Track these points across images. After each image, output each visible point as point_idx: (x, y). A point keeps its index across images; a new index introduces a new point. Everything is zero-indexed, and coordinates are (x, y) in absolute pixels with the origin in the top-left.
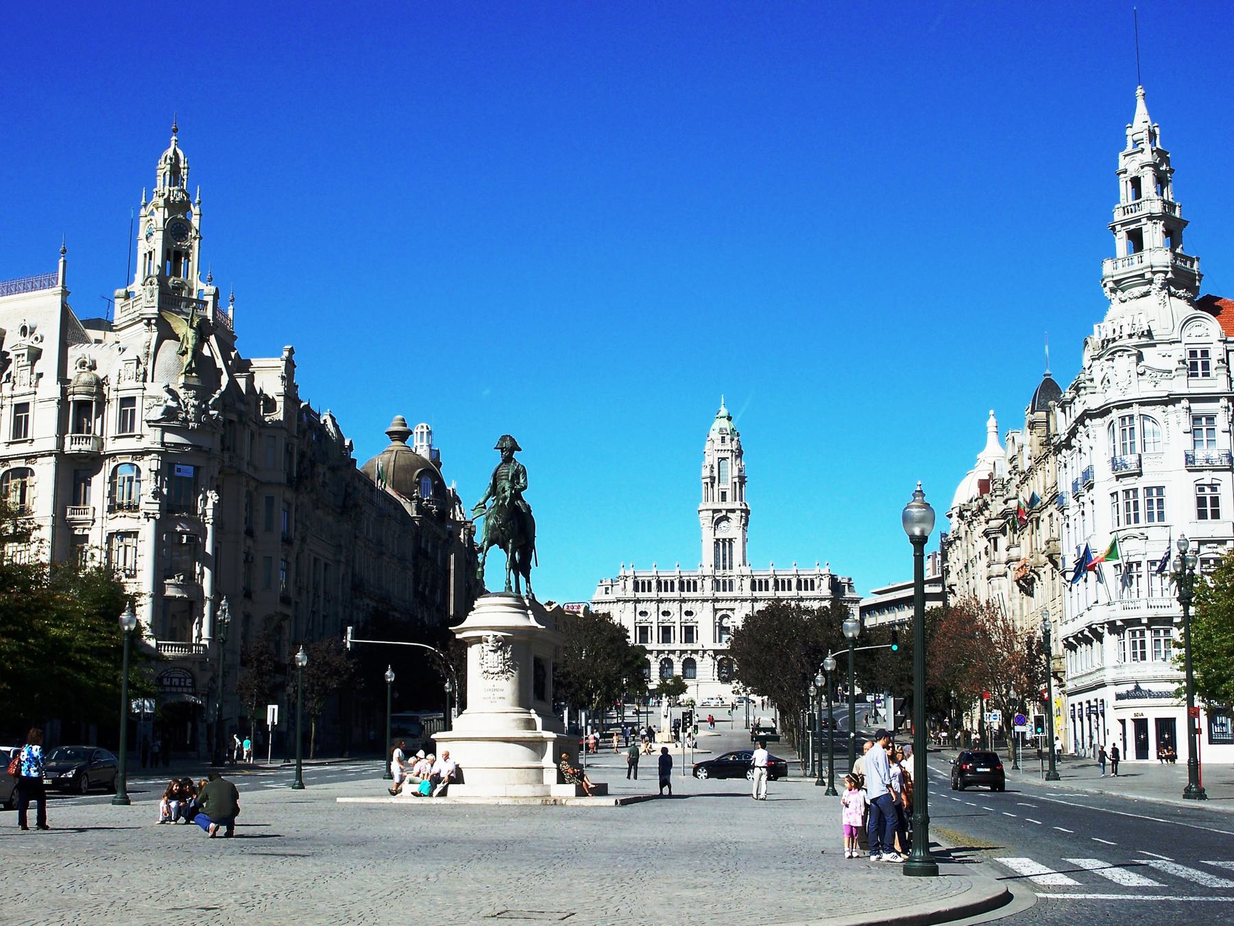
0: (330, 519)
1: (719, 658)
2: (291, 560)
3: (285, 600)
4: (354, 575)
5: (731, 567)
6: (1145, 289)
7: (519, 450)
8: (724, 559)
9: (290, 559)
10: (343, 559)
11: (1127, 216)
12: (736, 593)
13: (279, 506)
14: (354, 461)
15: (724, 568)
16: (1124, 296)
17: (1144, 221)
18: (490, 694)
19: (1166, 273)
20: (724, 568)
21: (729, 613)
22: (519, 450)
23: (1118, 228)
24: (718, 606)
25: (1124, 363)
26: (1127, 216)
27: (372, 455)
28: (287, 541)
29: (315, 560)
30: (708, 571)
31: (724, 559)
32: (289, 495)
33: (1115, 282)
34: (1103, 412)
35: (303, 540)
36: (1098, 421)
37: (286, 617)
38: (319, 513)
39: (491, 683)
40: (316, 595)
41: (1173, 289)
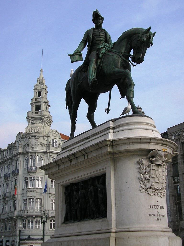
6: (41, 121)
11: (36, 101)
16: (33, 122)
17: (42, 103)
19: (47, 118)
23: (33, 104)
25: (33, 141)
26: (36, 101)
33: (32, 118)
34: (25, 154)
36: (23, 156)
41: (47, 123)
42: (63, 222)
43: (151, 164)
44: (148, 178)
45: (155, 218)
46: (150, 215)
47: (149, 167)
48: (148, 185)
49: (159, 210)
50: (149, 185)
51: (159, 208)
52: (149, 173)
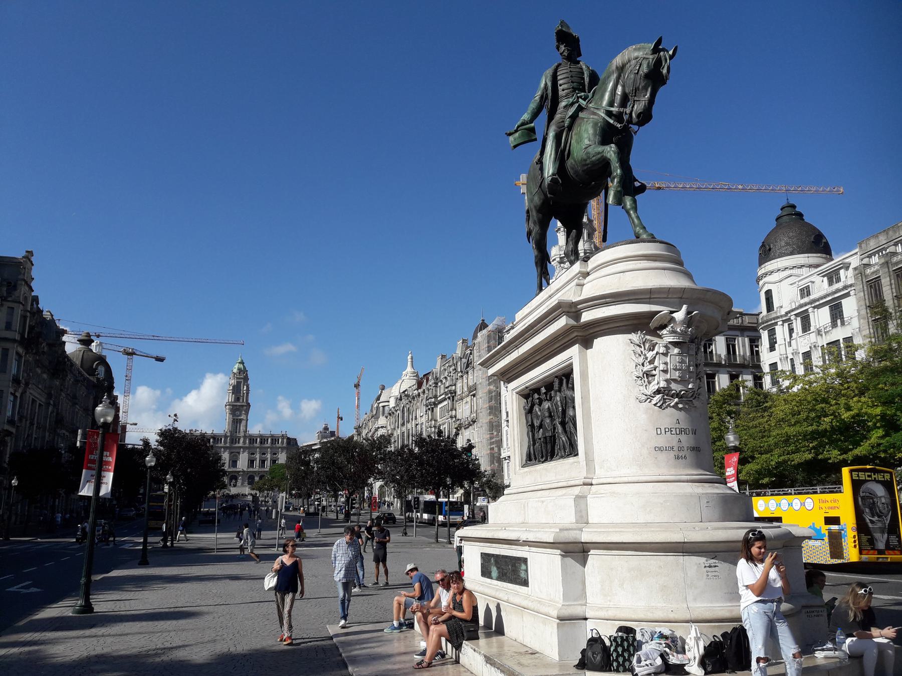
0: (45, 376)
2: (18, 394)
3: (11, 422)
4: (57, 414)
9: (18, 394)
10: (52, 402)
12: (241, 444)
13: (13, 356)
14: (64, 342)
27: (71, 346)
28: (16, 381)
29: (33, 401)
30: (228, 434)
32: (20, 350)
35: (27, 384)
37: (9, 433)
38: (39, 371)
40: (32, 424)
42: (524, 462)
44: (654, 372)
46: (660, 449)
48: (654, 387)
50: (657, 387)
52: (652, 362)
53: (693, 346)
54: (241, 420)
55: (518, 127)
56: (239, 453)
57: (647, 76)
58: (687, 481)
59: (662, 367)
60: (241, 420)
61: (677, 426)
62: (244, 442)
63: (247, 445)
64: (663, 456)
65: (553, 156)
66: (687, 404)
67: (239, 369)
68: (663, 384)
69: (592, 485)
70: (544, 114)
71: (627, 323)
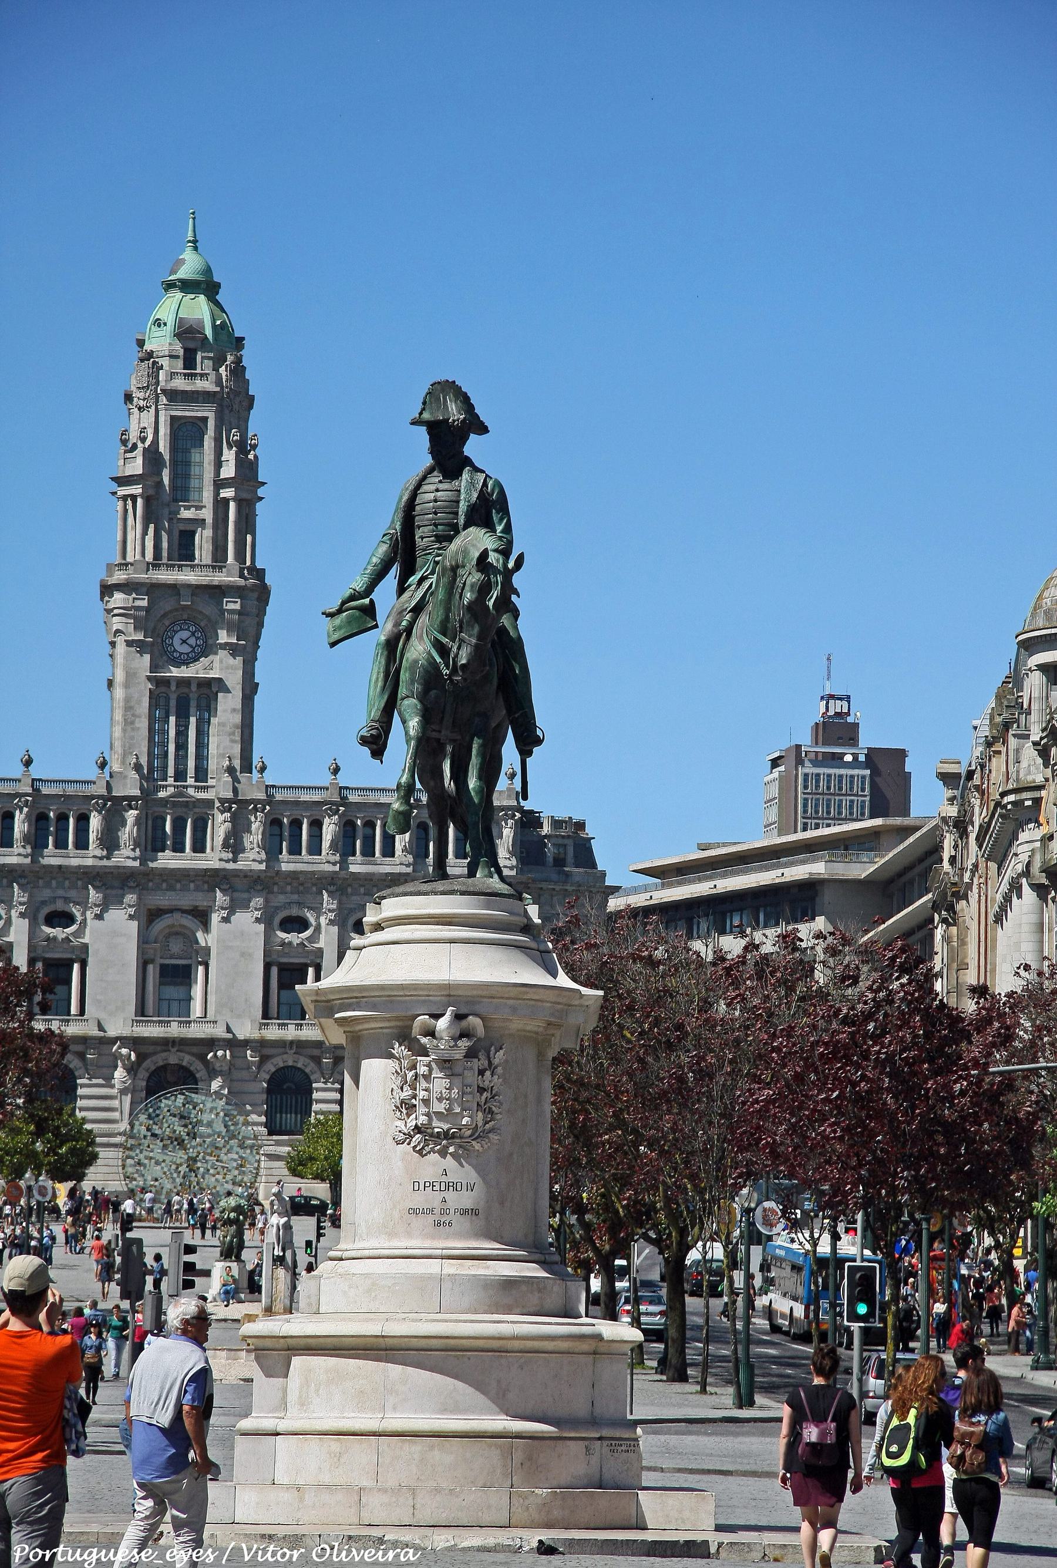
1: (149, 1064)
5: (201, 774)
7: (483, 429)
8: (181, 746)
15: (180, 775)
18: (434, 1199)
20: (180, 775)
21: (187, 921)
22: (483, 429)
24: (162, 899)
30: (130, 787)
31: (181, 746)
39: (434, 1165)
43: (419, 1058)
45: (431, 1219)
46: (414, 1211)
47: (414, 1067)
49: (450, 1195)
50: (414, 1123)
51: (451, 1188)
53: (476, 1064)
54: (209, 691)
55: (343, 603)
56: (202, 917)
57: (470, 607)
58: (442, 1258)
59: (422, 1094)
60: (209, 691)
61: (444, 1178)
62: (234, 844)
63: (252, 859)
64: (418, 1222)
65: (380, 684)
66: (461, 1147)
67: (187, 334)
68: (423, 1120)
69: (341, 1259)
70: (395, 571)
71: (387, 1024)
